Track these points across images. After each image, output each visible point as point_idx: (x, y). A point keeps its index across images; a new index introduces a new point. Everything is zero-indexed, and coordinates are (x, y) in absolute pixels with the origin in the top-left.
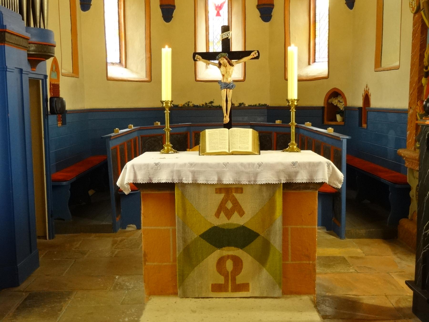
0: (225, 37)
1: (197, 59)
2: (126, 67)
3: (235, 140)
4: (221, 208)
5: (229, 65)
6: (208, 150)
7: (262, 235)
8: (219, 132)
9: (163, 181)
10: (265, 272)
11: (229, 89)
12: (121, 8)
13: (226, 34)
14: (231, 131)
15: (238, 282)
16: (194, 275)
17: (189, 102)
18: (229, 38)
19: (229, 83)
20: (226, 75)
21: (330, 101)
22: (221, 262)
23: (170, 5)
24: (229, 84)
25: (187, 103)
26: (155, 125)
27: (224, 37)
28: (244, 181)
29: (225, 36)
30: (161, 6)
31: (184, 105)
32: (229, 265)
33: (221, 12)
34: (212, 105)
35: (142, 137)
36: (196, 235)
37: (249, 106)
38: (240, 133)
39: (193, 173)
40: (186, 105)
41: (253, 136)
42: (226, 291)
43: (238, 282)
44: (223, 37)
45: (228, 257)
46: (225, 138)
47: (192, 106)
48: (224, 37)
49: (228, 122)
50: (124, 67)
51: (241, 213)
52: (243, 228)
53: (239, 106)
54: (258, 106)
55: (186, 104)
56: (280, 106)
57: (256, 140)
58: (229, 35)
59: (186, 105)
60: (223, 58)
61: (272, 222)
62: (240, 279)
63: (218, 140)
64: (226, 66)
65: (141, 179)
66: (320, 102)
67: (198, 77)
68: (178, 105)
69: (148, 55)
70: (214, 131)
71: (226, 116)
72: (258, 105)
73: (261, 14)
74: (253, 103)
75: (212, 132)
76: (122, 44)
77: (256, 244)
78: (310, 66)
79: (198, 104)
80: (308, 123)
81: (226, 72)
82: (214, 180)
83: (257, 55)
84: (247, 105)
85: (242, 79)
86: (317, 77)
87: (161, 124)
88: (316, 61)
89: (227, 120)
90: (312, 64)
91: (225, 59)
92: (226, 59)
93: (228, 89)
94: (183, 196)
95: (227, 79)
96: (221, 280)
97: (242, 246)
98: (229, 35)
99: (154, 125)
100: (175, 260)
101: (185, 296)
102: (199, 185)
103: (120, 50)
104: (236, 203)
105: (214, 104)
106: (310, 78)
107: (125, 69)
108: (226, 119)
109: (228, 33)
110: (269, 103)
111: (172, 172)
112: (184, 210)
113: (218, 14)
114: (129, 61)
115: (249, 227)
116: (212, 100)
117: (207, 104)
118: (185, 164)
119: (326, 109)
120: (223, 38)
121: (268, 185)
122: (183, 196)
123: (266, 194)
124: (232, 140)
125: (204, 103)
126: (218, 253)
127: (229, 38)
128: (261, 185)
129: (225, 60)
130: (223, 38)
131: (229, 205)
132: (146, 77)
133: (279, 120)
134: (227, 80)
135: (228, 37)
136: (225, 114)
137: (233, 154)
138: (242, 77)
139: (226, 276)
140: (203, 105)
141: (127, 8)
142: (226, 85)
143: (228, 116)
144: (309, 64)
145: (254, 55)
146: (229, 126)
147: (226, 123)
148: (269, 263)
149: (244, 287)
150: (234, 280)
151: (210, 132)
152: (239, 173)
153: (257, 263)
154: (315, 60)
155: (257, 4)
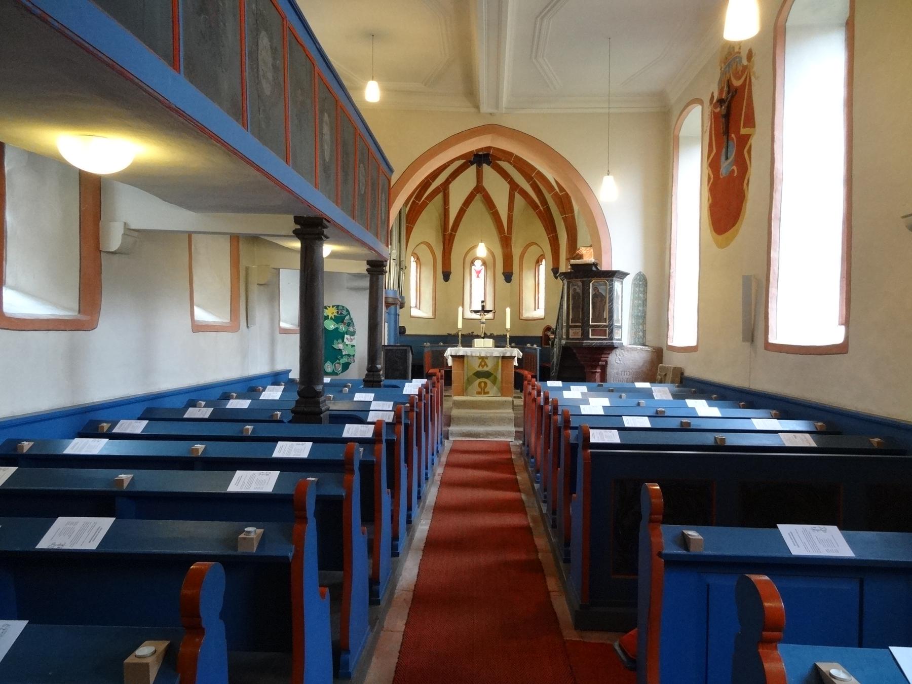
2: (419, 309)
6: (476, 346)
9: (461, 354)
10: (495, 387)
15: (486, 391)
16: (470, 388)
21: (546, 333)
22: (480, 383)
28: (488, 355)
30: (443, 272)
32: (483, 385)
33: (480, 275)
35: (432, 351)
36: (471, 374)
39: (471, 352)
41: (493, 342)
42: (481, 394)
43: (486, 391)
51: (487, 366)
52: (487, 371)
61: (498, 370)
62: (486, 390)
65: (453, 354)
66: (539, 333)
69: (434, 302)
73: (505, 278)
77: (492, 378)
82: (478, 355)
85: (493, 318)
94: (467, 360)
96: (480, 390)
97: (487, 378)
100: (464, 383)
102: (473, 356)
104: (485, 363)
105: (474, 334)
111: (464, 352)
112: (467, 365)
113: (478, 277)
114: (421, 307)
119: (543, 338)
121: (496, 356)
122: (467, 360)
123: (495, 360)
125: (468, 333)
126: (479, 380)
131: (483, 364)
137: (485, 348)
139: (482, 389)
144: (535, 310)
148: (496, 385)
149: (488, 393)
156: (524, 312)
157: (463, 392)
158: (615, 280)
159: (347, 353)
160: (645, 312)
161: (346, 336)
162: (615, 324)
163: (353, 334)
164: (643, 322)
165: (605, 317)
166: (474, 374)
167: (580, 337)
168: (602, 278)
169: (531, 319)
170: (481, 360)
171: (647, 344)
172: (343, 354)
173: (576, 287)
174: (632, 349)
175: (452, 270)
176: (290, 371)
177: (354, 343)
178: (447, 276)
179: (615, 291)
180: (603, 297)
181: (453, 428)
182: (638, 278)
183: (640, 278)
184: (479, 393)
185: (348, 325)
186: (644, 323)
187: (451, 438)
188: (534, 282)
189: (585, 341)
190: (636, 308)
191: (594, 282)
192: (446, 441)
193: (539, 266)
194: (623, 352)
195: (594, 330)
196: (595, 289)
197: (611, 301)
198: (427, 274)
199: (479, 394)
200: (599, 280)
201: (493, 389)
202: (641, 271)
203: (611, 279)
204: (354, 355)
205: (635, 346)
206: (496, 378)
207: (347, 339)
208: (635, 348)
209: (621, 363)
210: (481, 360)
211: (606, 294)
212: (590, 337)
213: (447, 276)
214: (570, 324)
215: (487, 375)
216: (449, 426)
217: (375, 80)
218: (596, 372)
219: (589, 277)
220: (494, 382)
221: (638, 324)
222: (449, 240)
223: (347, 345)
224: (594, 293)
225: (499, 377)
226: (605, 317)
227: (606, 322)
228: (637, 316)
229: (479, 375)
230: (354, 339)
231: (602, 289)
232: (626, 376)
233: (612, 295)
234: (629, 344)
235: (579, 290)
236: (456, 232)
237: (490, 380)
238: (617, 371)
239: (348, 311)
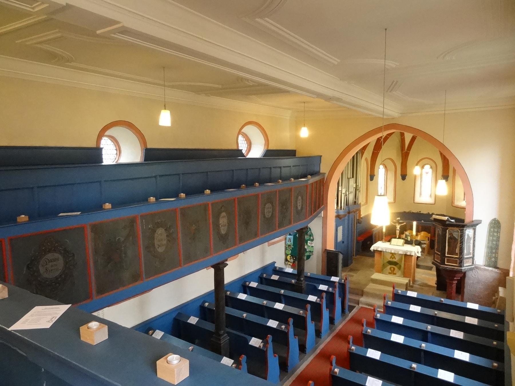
4: (391, 257)
6: (391, 244)
7: (400, 264)
16: (384, 270)
22: (390, 268)
28: (396, 252)
30: (401, 175)
32: (392, 269)
36: (386, 262)
39: (386, 249)
45: (393, 267)
51: (395, 259)
62: (394, 272)
77: (398, 265)
82: (390, 252)
85: (434, 203)
89: (397, 237)
96: (390, 272)
101: (383, 273)
111: (381, 248)
115: (397, 262)
116: (420, 211)
118: (384, 248)
125: (417, 212)
126: (390, 266)
128: (400, 254)
131: (393, 257)
139: (392, 271)
146: (398, 238)
149: (395, 274)
150: (393, 272)
152: (395, 251)
153: (398, 270)
156: (455, 201)
157: (381, 271)
158: (466, 230)
159: (309, 250)
160: (497, 245)
161: (308, 242)
162: (465, 257)
163: (312, 240)
164: (496, 252)
165: (457, 252)
166: (387, 262)
167: (439, 262)
168: (455, 228)
169: (459, 207)
170: (391, 255)
171: (498, 266)
172: (307, 251)
173: (439, 230)
174: (485, 270)
175: (408, 174)
176: (275, 263)
177: (313, 245)
178: (404, 177)
179: (466, 237)
180: (455, 240)
181: (363, 299)
182: (493, 222)
183: (495, 223)
184: (390, 273)
185: (310, 236)
186: (496, 253)
187: (360, 305)
189: (442, 266)
190: (491, 242)
191: (450, 229)
192: (357, 306)
194: (478, 271)
195: (448, 259)
196: (450, 234)
197: (462, 242)
198: (391, 175)
199: (390, 274)
200: (452, 228)
201: (399, 273)
202: (496, 218)
203: (462, 228)
204: (313, 251)
205: (487, 268)
206: (400, 266)
207: (309, 243)
208: (487, 269)
209: (476, 277)
210: (391, 255)
211: (458, 238)
212: (446, 263)
213: (404, 177)
214: (436, 252)
215: (395, 264)
216: (362, 295)
217: (305, 127)
218: (453, 283)
219: (446, 227)
220: (400, 268)
221: (492, 253)
223: (309, 246)
224: (450, 236)
225: (403, 266)
226: (457, 252)
227: (457, 256)
228: (491, 247)
229: (390, 263)
230: (313, 243)
231: (456, 235)
232: (481, 287)
233: (463, 238)
234: (484, 264)
235: (440, 233)
237: (397, 267)
238: (473, 282)
239: (310, 229)
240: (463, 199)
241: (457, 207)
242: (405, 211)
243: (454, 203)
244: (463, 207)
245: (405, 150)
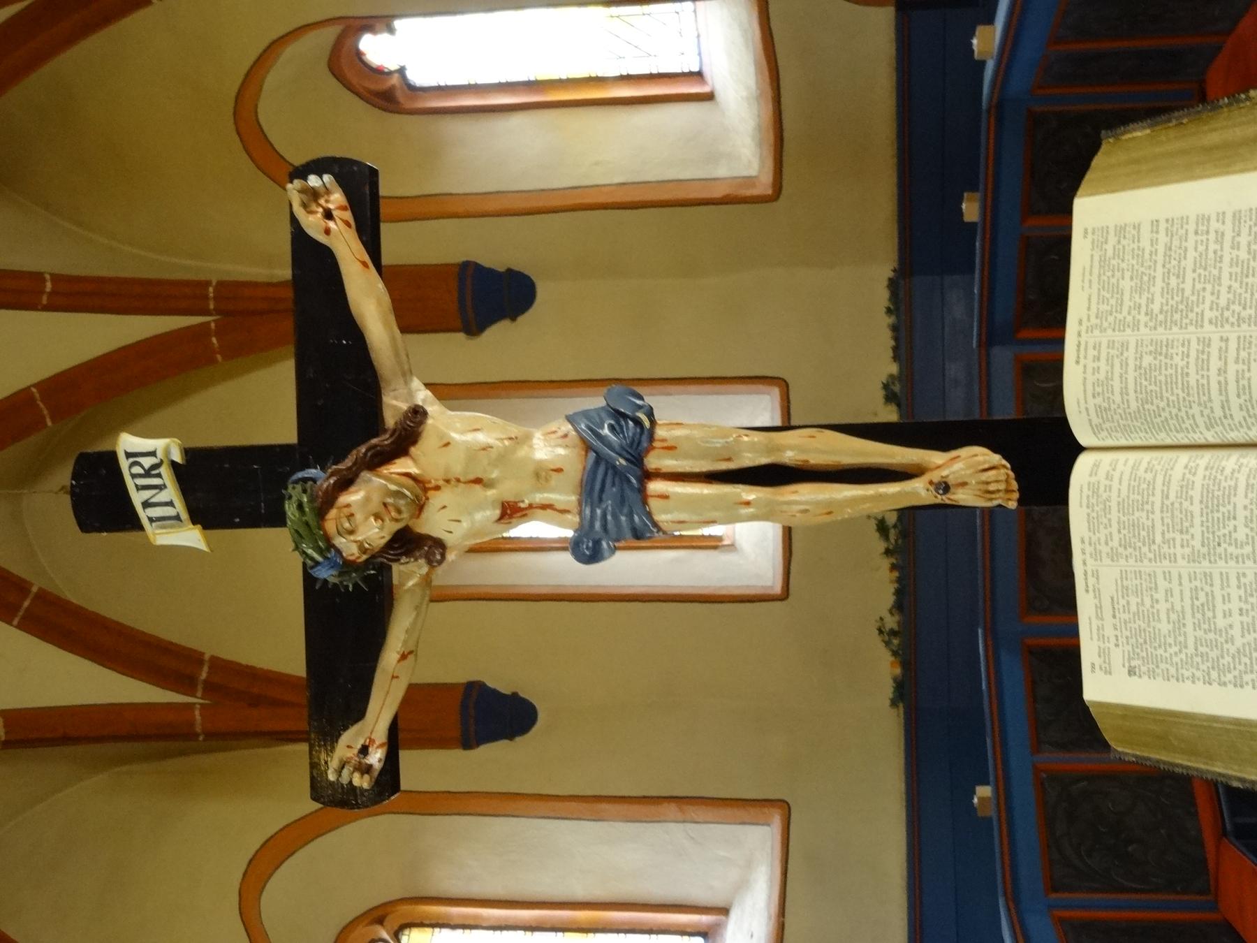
0: (171, 492)
1: (367, 769)
2: (725, 911)
3: (1222, 371)
5: (413, 450)
8: (1114, 556)
11: (650, 448)
12: (476, 917)
13: (140, 488)
14: (1097, 430)
17: (881, 631)
18: (177, 457)
19: (588, 447)
20: (507, 490)
23: (464, 706)
24: (592, 455)
25: (887, 638)
26: (991, 812)
27: (170, 504)
29: (163, 496)
30: (468, 743)
31: (895, 653)
34: (895, 526)
35: (1054, 886)
37: (896, 358)
38: (1121, 326)
40: (896, 642)
44: (168, 511)
46: (1196, 494)
47: (897, 618)
48: (170, 504)
49: (996, 458)
50: (722, 918)
53: (899, 405)
54: (898, 316)
55: (887, 644)
56: (896, 217)
57: (1213, 138)
58: (147, 462)
59: (896, 642)
60: (333, 513)
63: (1224, 578)
64: (422, 488)
67: (772, 587)
68: (895, 680)
69: (672, 809)
70: (1099, 607)
71: (936, 476)
72: (891, 320)
74: (886, 340)
75: (1109, 632)
76: (624, 923)
78: (717, 94)
79: (891, 588)
80: (975, 41)
81: (478, 481)
83: (327, 178)
84: (894, 369)
85: (776, 392)
86: (759, 46)
87: (987, 783)
88: (696, 69)
90: (710, 81)
91: (344, 499)
92: (346, 483)
93: (654, 461)
95: (543, 474)
98: (153, 454)
99: (990, 819)
103: (650, 931)
106: (768, 80)
107: (734, 914)
108: (964, 484)
109: (137, 470)
110: (883, 269)
117: (891, 547)
120: (177, 518)
124: (1225, 405)
125: (886, 563)
127: (177, 457)
129: (353, 497)
130: (184, 515)
132: (769, 825)
133: (964, 206)
134: (559, 470)
135: (174, 464)
136: (918, 491)
138: (768, 394)
140: (893, 567)
141: (476, 890)
142: (602, 490)
143: (935, 458)
144: (709, 97)
145: (328, 215)
147: (1015, 485)
151: (1117, 656)
154: (690, 75)
155: (461, 336)
156: (722, 172)
175: (459, 676)
188: (517, 120)
193: (412, 89)
222: (256, 701)
236: (195, 658)
240: (705, 105)
241: (770, 137)
242: (888, 690)
243: (749, 181)
244: (757, 64)
245: (190, 706)
